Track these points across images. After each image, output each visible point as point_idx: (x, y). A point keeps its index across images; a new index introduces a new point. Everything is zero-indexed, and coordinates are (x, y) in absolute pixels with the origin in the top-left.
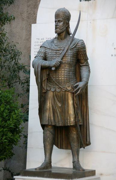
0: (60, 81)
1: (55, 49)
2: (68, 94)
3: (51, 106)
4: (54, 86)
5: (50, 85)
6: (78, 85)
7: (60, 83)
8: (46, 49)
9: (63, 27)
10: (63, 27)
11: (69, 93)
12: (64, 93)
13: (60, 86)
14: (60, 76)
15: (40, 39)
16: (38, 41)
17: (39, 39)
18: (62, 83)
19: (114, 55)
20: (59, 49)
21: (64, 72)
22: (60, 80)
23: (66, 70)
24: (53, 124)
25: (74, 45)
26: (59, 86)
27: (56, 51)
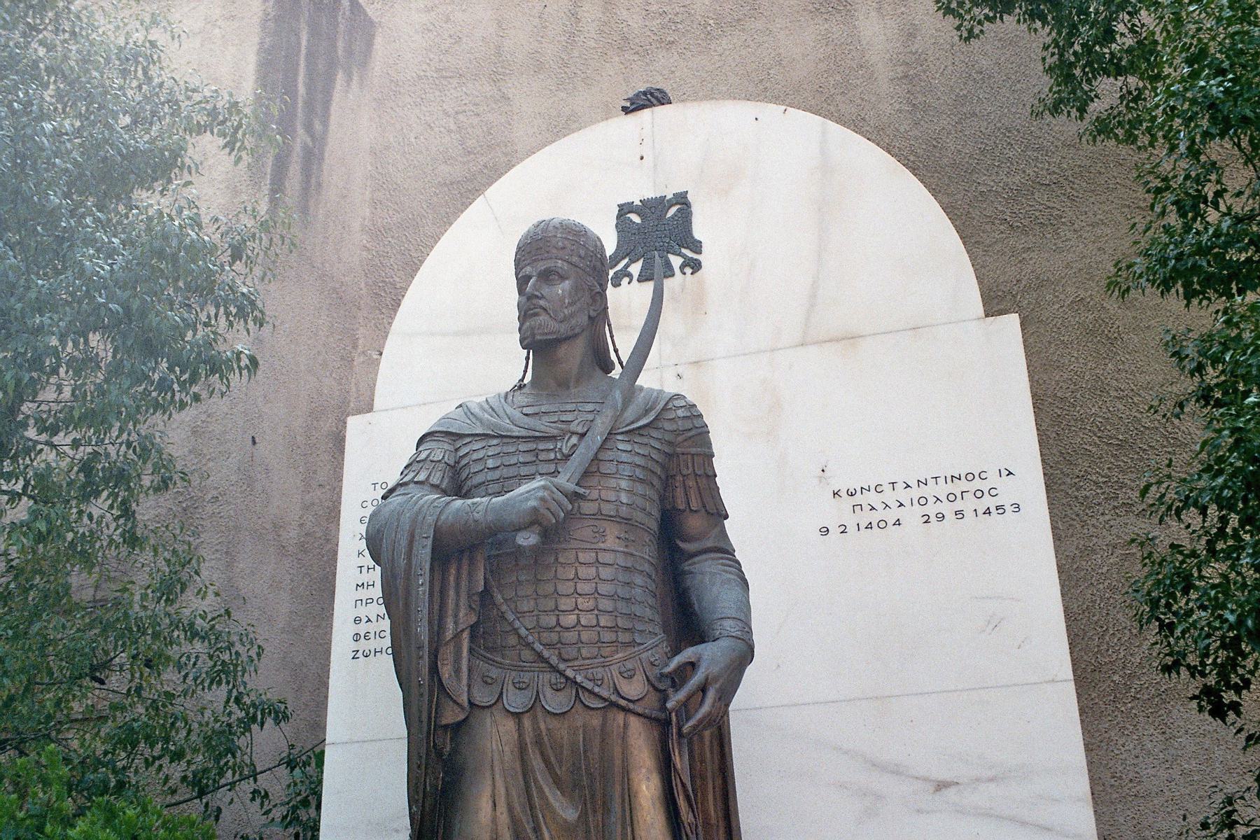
0: (570, 636)
1: (524, 433)
2: (626, 726)
3: (504, 818)
4: (526, 677)
5: (494, 673)
6: (693, 665)
7: (570, 652)
9: (573, 309)
10: (573, 309)
11: (635, 723)
12: (596, 721)
13: (570, 673)
14: (565, 604)
18: (584, 652)
20: (555, 432)
21: (592, 571)
23: (606, 558)
25: (647, 412)
26: (562, 674)
27: (532, 446)
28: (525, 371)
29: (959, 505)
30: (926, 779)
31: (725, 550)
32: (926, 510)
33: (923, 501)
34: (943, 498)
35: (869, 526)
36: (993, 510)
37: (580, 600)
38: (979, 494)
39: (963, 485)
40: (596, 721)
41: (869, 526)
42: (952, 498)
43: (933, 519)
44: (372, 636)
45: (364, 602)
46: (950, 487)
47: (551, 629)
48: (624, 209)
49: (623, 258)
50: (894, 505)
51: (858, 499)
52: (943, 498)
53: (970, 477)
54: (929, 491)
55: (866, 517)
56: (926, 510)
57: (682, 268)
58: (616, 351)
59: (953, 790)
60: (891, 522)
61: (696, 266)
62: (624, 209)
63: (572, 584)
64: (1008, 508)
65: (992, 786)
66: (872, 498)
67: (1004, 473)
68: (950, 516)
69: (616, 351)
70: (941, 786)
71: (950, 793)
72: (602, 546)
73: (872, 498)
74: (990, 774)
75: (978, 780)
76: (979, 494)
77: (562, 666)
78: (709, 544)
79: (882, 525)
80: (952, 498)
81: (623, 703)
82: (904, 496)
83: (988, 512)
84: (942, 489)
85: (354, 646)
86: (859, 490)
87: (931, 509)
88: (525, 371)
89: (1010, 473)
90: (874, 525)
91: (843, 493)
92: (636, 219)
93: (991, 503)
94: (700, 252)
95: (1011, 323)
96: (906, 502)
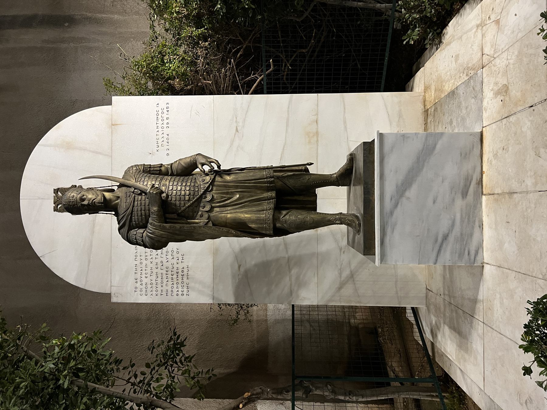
5: (200, 213)
13: (201, 192)
14: (183, 193)
16: (138, 290)
17: (136, 288)
22: (190, 194)
29: (165, 118)
32: (165, 127)
34: (163, 122)
36: (167, 110)
38: (163, 113)
39: (159, 117)
42: (163, 120)
43: (168, 125)
44: (182, 290)
46: (160, 120)
47: (189, 198)
48: (56, 210)
50: (163, 135)
51: (160, 145)
53: (158, 115)
54: (160, 126)
55: (165, 143)
56: (165, 127)
58: (109, 186)
59: (238, 128)
62: (56, 210)
64: (168, 106)
65: (238, 118)
66: (160, 141)
67: (158, 106)
68: (167, 121)
69: (109, 186)
70: (237, 130)
72: (168, 185)
74: (235, 118)
76: (163, 113)
78: (169, 167)
80: (163, 120)
81: (211, 181)
82: (160, 133)
84: (160, 122)
87: (165, 125)
89: (158, 104)
93: (165, 110)
95: (114, 99)
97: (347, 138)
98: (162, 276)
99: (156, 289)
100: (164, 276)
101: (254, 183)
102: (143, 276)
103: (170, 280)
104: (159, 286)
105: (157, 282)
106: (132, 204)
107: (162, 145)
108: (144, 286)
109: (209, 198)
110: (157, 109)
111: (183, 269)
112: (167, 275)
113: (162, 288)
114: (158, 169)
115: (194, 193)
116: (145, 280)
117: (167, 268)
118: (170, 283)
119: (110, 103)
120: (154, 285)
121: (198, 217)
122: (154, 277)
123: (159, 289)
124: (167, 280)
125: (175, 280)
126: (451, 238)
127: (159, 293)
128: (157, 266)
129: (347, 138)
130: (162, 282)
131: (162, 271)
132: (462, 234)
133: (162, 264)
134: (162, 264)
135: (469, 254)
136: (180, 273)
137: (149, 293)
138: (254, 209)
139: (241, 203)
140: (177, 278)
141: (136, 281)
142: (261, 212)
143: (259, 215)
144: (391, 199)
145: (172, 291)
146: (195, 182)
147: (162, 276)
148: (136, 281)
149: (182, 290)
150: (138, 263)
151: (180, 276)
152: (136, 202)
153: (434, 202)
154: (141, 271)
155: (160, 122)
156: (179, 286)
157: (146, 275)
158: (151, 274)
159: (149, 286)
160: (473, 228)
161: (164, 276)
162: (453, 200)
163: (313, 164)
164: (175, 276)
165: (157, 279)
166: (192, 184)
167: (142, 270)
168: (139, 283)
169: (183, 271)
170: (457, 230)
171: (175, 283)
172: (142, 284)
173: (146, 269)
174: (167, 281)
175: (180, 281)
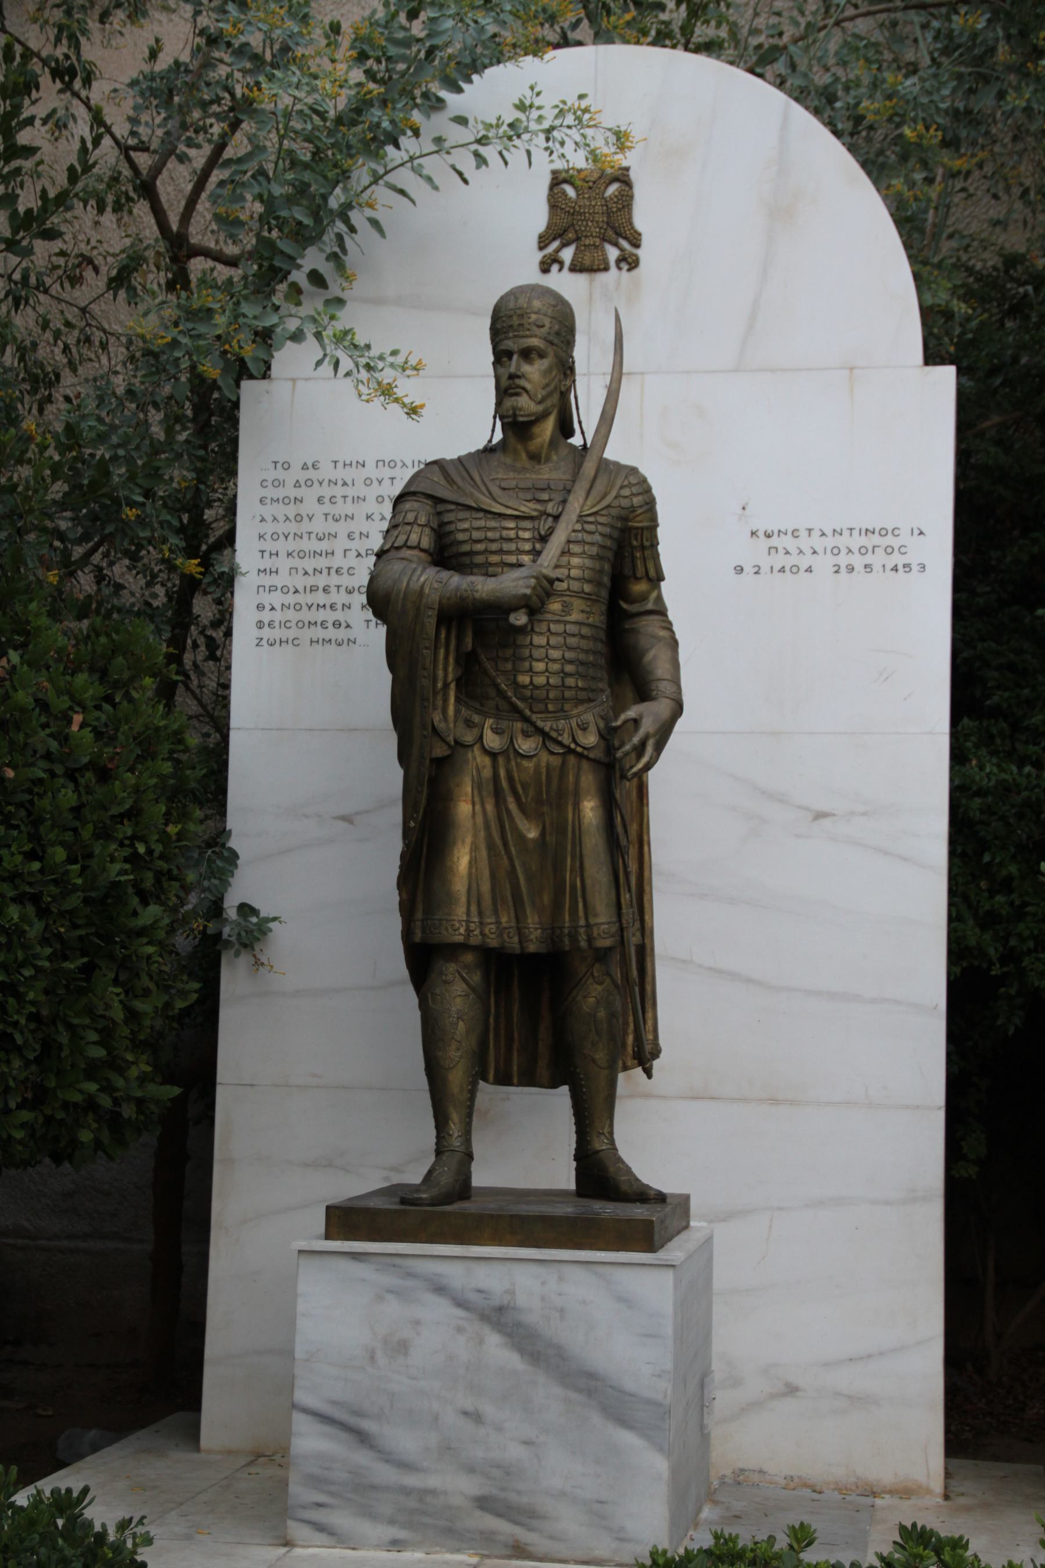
4: (504, 724)
5: (476, 718)
6: (636, 722)
8: (441, 508)
12: (556, 761)
13: (540, 724)
14: (540, 666)
15: (296, 466)
16: (280, 474)
17: (287, 466)
19: (748, 569)
20: (535, 514)
21: (561, 639)
22: (537, 687)
24: (493, 942)
26: (533, 724)
28: (493, 431)
30: (807, 809)
31: (661, 612)
33: (836, 551)
34: (855, 550)
35: (782, 570)
36: (900, 567)
37: (550, 664)
38: (889, 551)
39: (876, 539)
40: (556, 761)
41: (782, 570)
42: (863, 551)
43: (843, 570)
44: (277, 624)
45: (267, 589)
46: (863, 541)
47: (525, 687)
49: (554, 239)
50: (808, 551)
51: (774, 541)
52: (855, 550)
53: (883, 532)
54: (843, 541)
55: (780, 560)
57: (618, 262)
58: (580, 423)
60: (803, 567)
61: (630, 262)
63: (543, 650)
64: (915, 568)
66: (787, 542)
67: (916, 532)
69: (580, 423)
70: (820, 816)
71: (826, 823)
72: (568, 618)
73: (787, 542)
75: (853, 813)
76: (889, 551)
77: (534, 717)
78: (650, 606)
79: (795, 569)
80: (863, 551)
81: (579, 749)
83: (895, 569)
84: (857, 541)
85: (256, 633)
86: (776, 533)
87: (843, 560)
88: (493, 431)
89: (921, 533)
90: (787, 569)
91: (761, 534)
92: (570, 192)
93: (897, 559)
94: (637, 245)
95: (949, 373)
96: (820, 550)
97: (781, 1209)
98: (324, 554)
99: (281, 536)
100: (322, 563)
101: (573, 887)
102: (326, 492)
103: (310, 581)
104: (292, 545)
105: (306, 536)
106: (509, 512)
107: (773, 551)
108: (293, 493)
109: (525, 745)
110: (905, 532)
111: (344, 625)
112: (325, 571)
113: (283, 554)
114: (640, 572)
115: (540, 701)
116: (310, 495)
117: (351, 571)
118: (300, 581)
119: (932, 357)
120: (292, 527)
121: (465, 712)
122: (319, 526)
123: (282, 546)
124: (311, 572)
125: (310, 598)
126: (362, 1458)
127: (269, 545)
128: (357, 535)
129: (781, 1209)
130: (302, 555)
131: (339, 553)
132: (374, 1487)
133: (364, 554)
134: (364, 554)
135: (320, 1505)
136: (330, 616)
137: (268, 511)
138: (486, 887)
139: (505, 844)
140: (315, 606)
141: (310, 465)
142: (474, 909)
143: (463, 899)
144: (480, 1291)
145: (273, 589)
146: (580, 702)
147: (324, 554)
148: (310, 465)
149: (277, 624)
150: (371, 471)
151: (321, 615)
152: (511, 524)
153: (466, 1413)
154: (340, 483)
155: (857, 541)
156: (291, 615)
157: (326, 500)
158: (330, 517)
159: (291, 510)
160: (392, 1522)
161: (322, 563)
162: (471, 1469)
163: (649, 1076)
164: (321, 598)
165: (313, 536)
166: (568, 694)
167: (345, 484)
168: (302, 476)
169: (337, 624)
170: (385, 1474)
171: (300, 598)
172: (297, 485)
173: (349, 500)
174: (306, 573)
175: (307, 616)
